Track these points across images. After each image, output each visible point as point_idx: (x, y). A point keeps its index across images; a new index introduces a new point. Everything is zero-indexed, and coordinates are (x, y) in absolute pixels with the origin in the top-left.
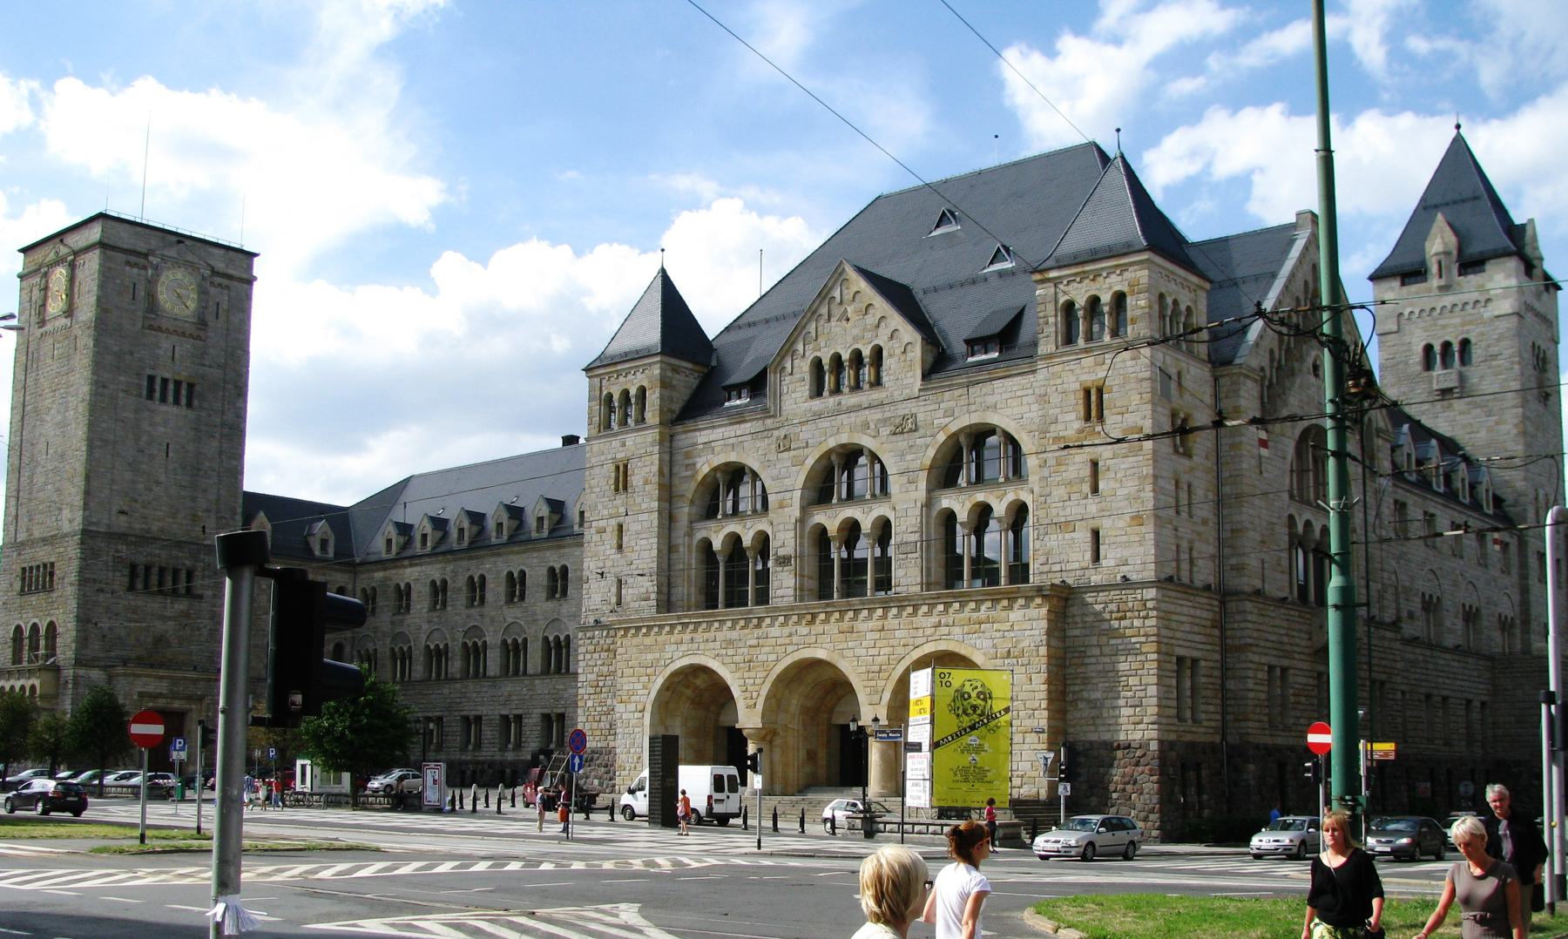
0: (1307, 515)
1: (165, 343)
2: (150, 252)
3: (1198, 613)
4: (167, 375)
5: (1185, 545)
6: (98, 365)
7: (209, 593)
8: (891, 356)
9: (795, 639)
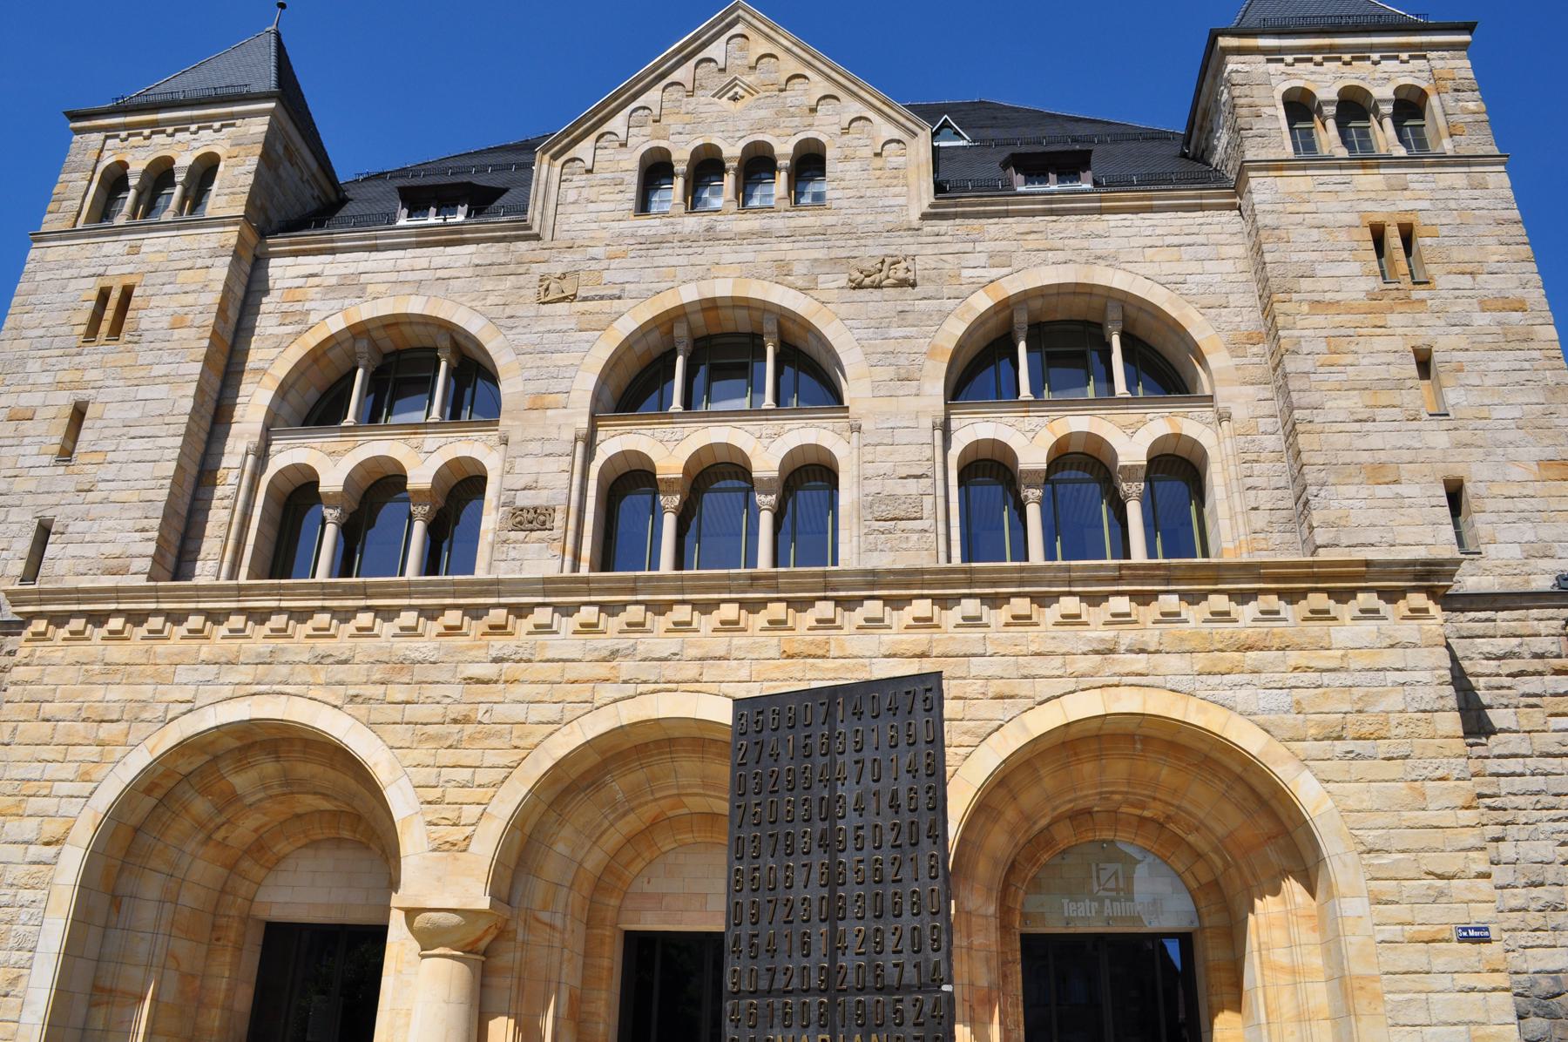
9: (626, 667)
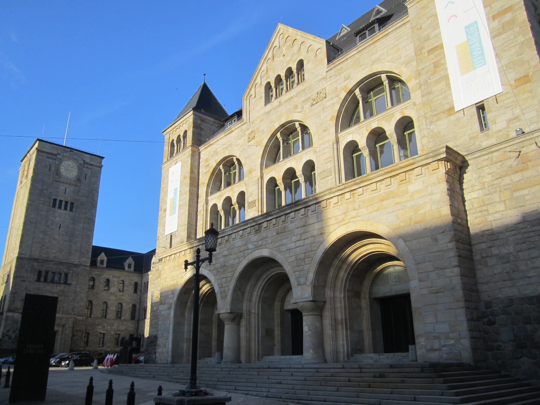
1: (62, 187)
2: (58, 154)
4: (62, 199)
6: (31, 193)
7: (75, 282)
8: (308, 62)
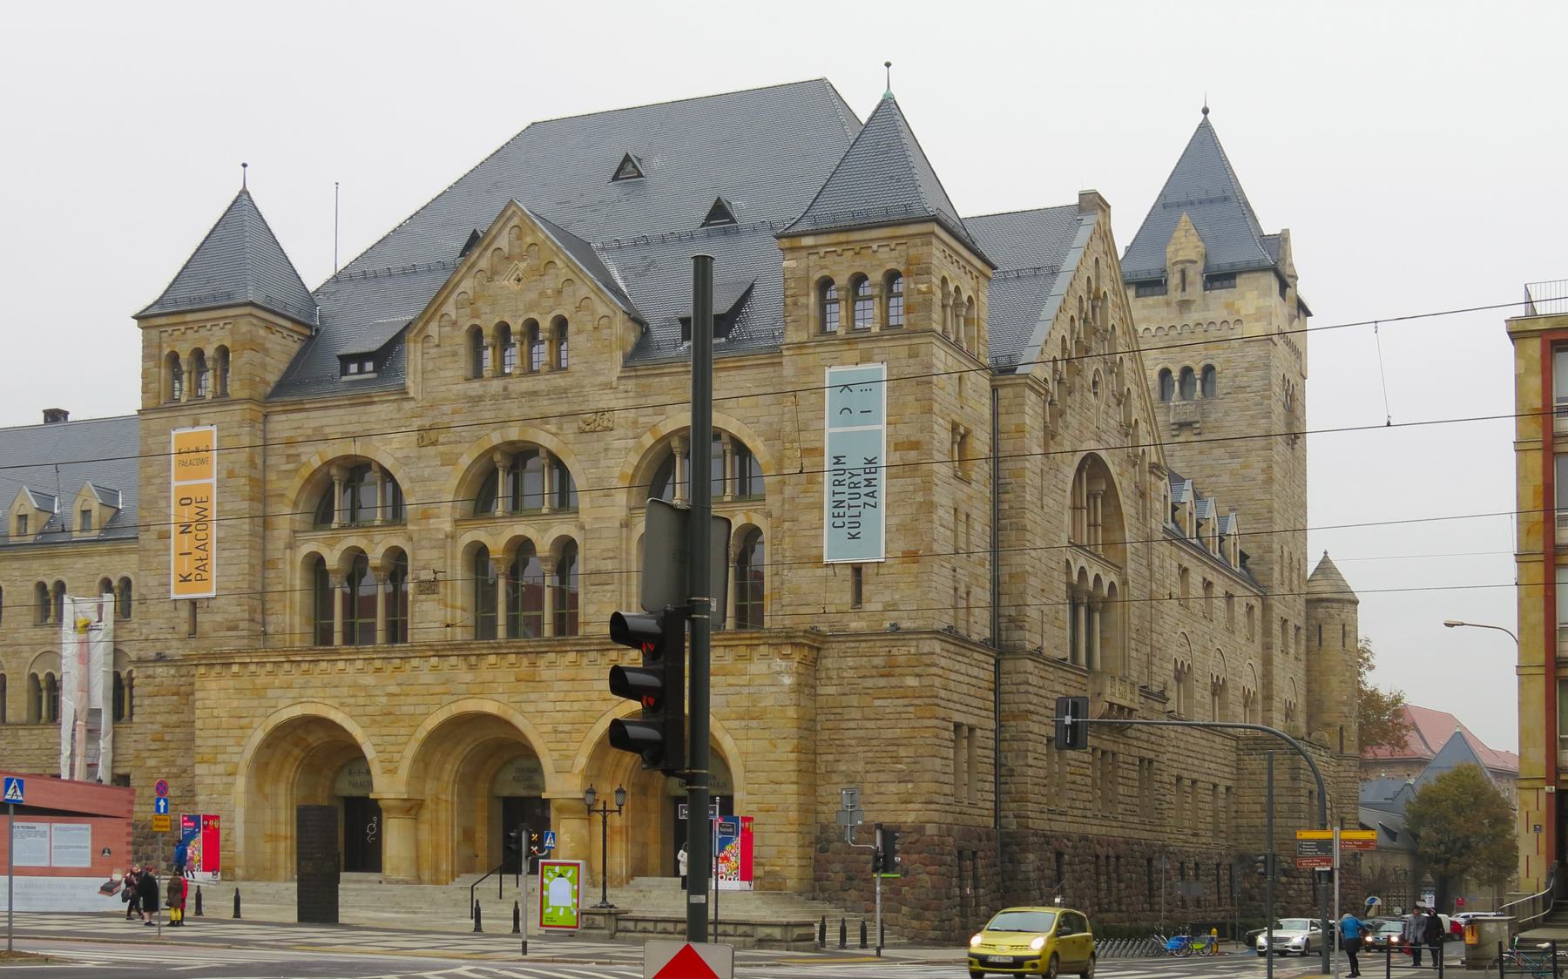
0: (1082, 562)
3: (975, 672)
5: (962, 590)
